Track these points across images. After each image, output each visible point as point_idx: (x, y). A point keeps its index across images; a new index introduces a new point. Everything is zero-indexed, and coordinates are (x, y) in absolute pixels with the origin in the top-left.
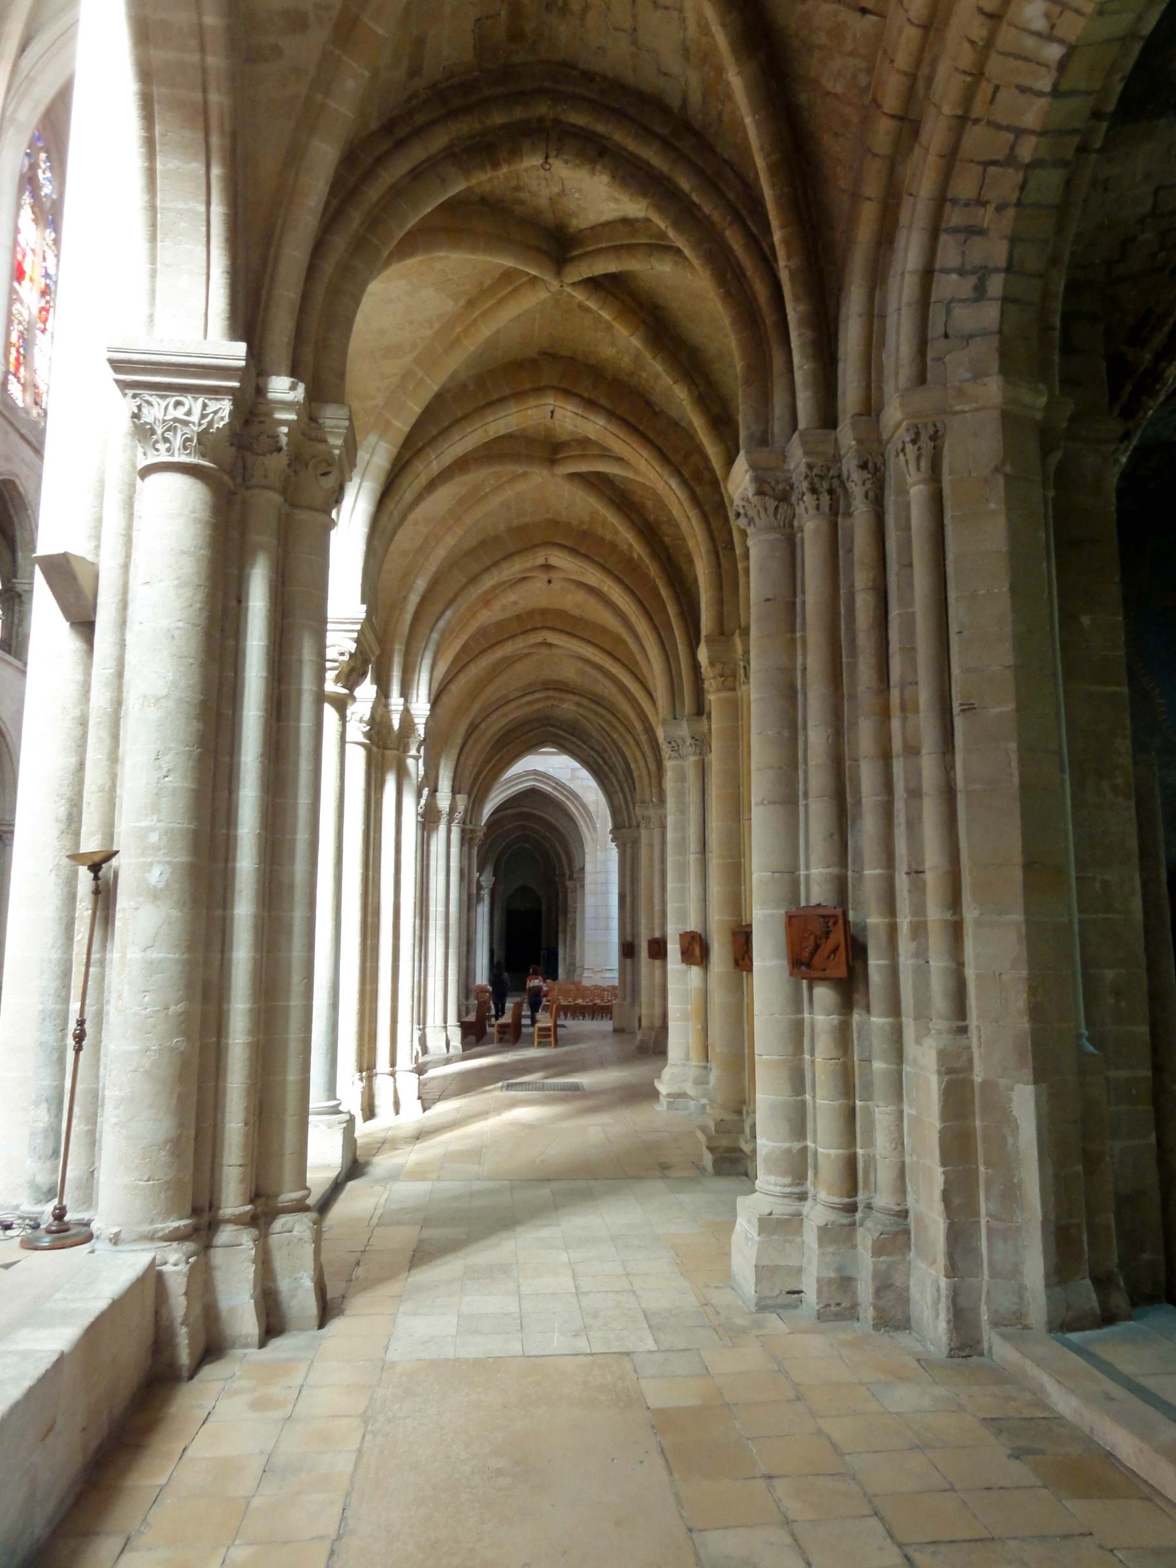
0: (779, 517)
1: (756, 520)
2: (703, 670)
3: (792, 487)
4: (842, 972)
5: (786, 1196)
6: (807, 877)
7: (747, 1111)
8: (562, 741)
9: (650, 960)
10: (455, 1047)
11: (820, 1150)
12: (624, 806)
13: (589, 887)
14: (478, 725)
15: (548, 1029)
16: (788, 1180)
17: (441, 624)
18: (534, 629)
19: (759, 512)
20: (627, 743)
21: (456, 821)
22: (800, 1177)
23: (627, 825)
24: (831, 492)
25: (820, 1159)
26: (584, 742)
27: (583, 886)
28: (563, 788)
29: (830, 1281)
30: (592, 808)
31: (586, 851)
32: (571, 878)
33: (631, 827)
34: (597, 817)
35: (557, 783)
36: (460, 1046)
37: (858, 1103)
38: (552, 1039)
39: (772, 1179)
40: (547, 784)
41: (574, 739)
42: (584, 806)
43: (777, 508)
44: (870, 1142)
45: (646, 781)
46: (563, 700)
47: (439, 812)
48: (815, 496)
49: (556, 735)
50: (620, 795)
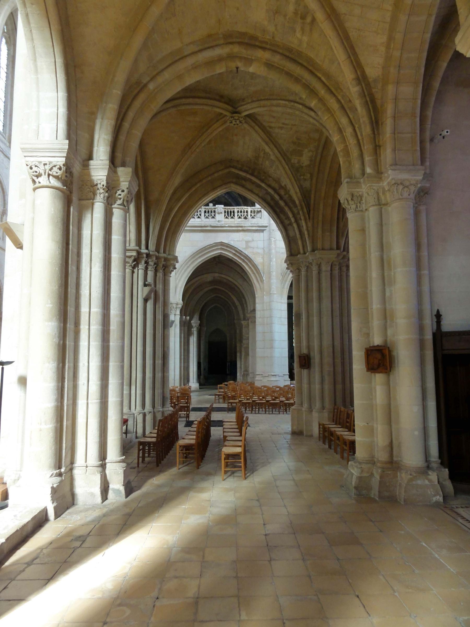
9: (369, 373)
10: (117, 491)
12: (298, 236)
13: (258, 320)
14: (146, 85)
15: (236, 456)
20: (328, 110)
21: (119, 202)
23: (302, 251)
26: (262, 181)
28: (240, 254)
30: (260, 267)
31: (256, 296)
35: (236, 251)
36: (122, 489)
38: (242, 465)
41: (254, 179)
45: (355, 153)
46: (249, 61)
47: (94, 186)
49: (238, 177)
50: (295, 225)
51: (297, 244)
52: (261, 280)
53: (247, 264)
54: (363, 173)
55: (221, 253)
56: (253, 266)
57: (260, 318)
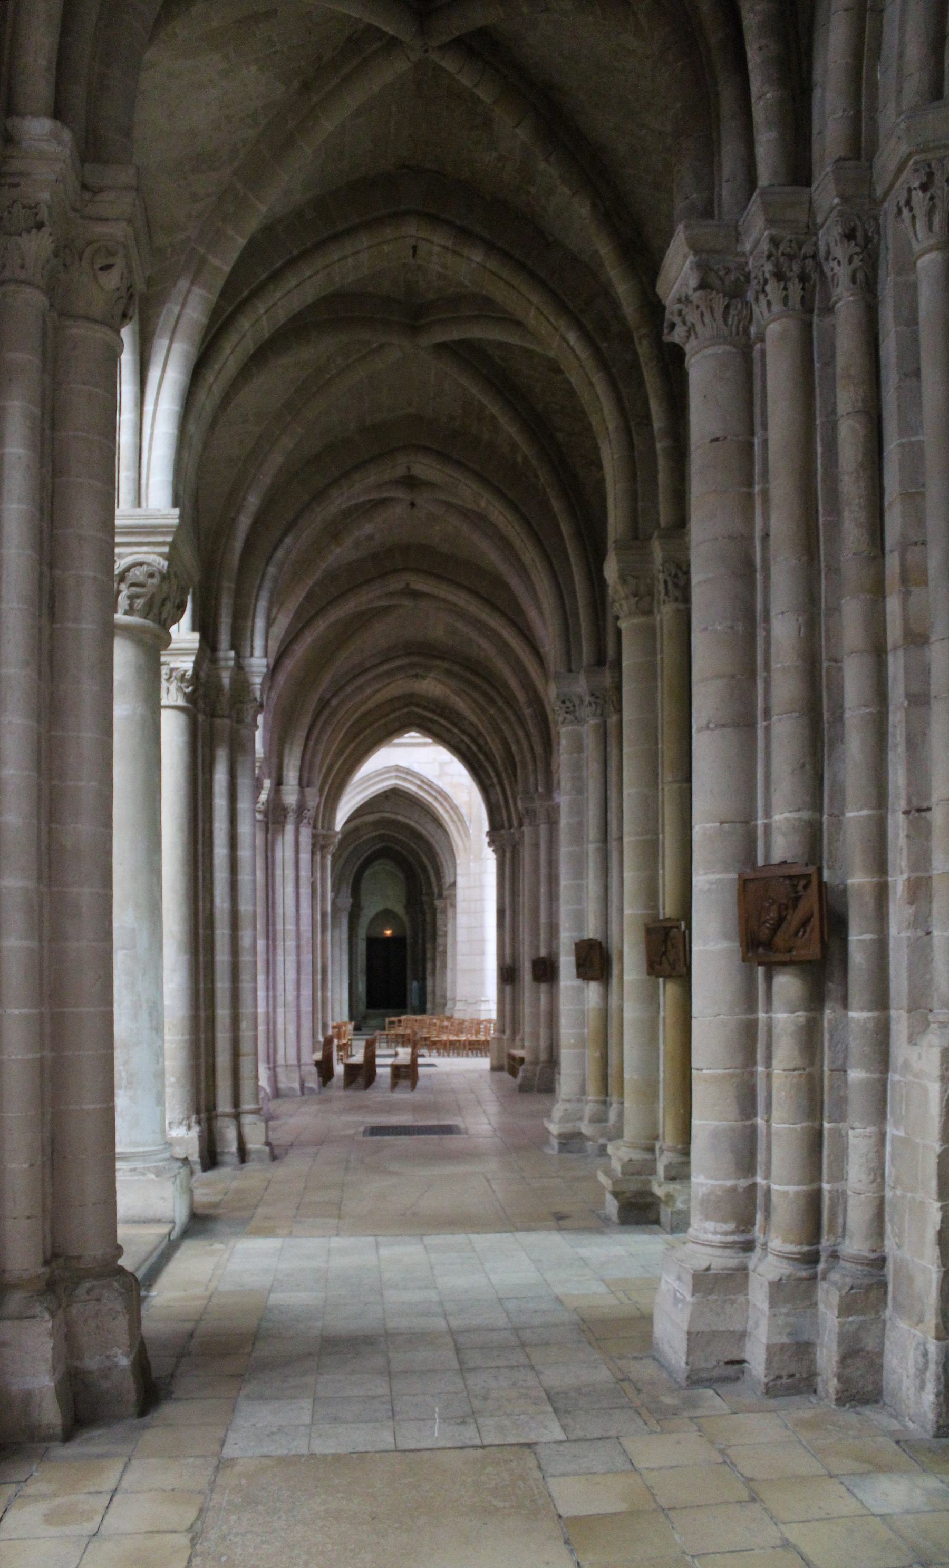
0: (730, 321)
1: (699, 327)
2: (610, 591)
3: (747, 276)
4: (814, 951)
5: (726, 1246)
6: (767, 827)
7: (661, 1149)
8: (430, 725)
11: (774, 1187)
13: (461, 905)
16: (731, 1226)
17: (280, 554)
18: (395, 571)
19: (702, 315)
20: (506, 719)
22: (745, 1222)
23: (506, 825)
24: (803, 278)
25: (774, 1198)
26: (455, 725)
27: (454, 906)
28: (430, 786)
29: (783, 1347)
30: (464, 810)
31: (458, 862)
32: (440, 895)
33: (511, 827)
34: (470, 821)
37: (826, 1125)
39: (710, 1225)
40: (411, 782)
41: (443, 721)
42: (455, 808)
43: (727, 307)
44: (839, 1175)
48: (782, 284)
50: (498, 788)
51: (501, 814)
52: (465, 833)
53: (441, 804)
54: (537, 789)
55: (396, 784)
56: (452, 808)
57: (464, 900)
